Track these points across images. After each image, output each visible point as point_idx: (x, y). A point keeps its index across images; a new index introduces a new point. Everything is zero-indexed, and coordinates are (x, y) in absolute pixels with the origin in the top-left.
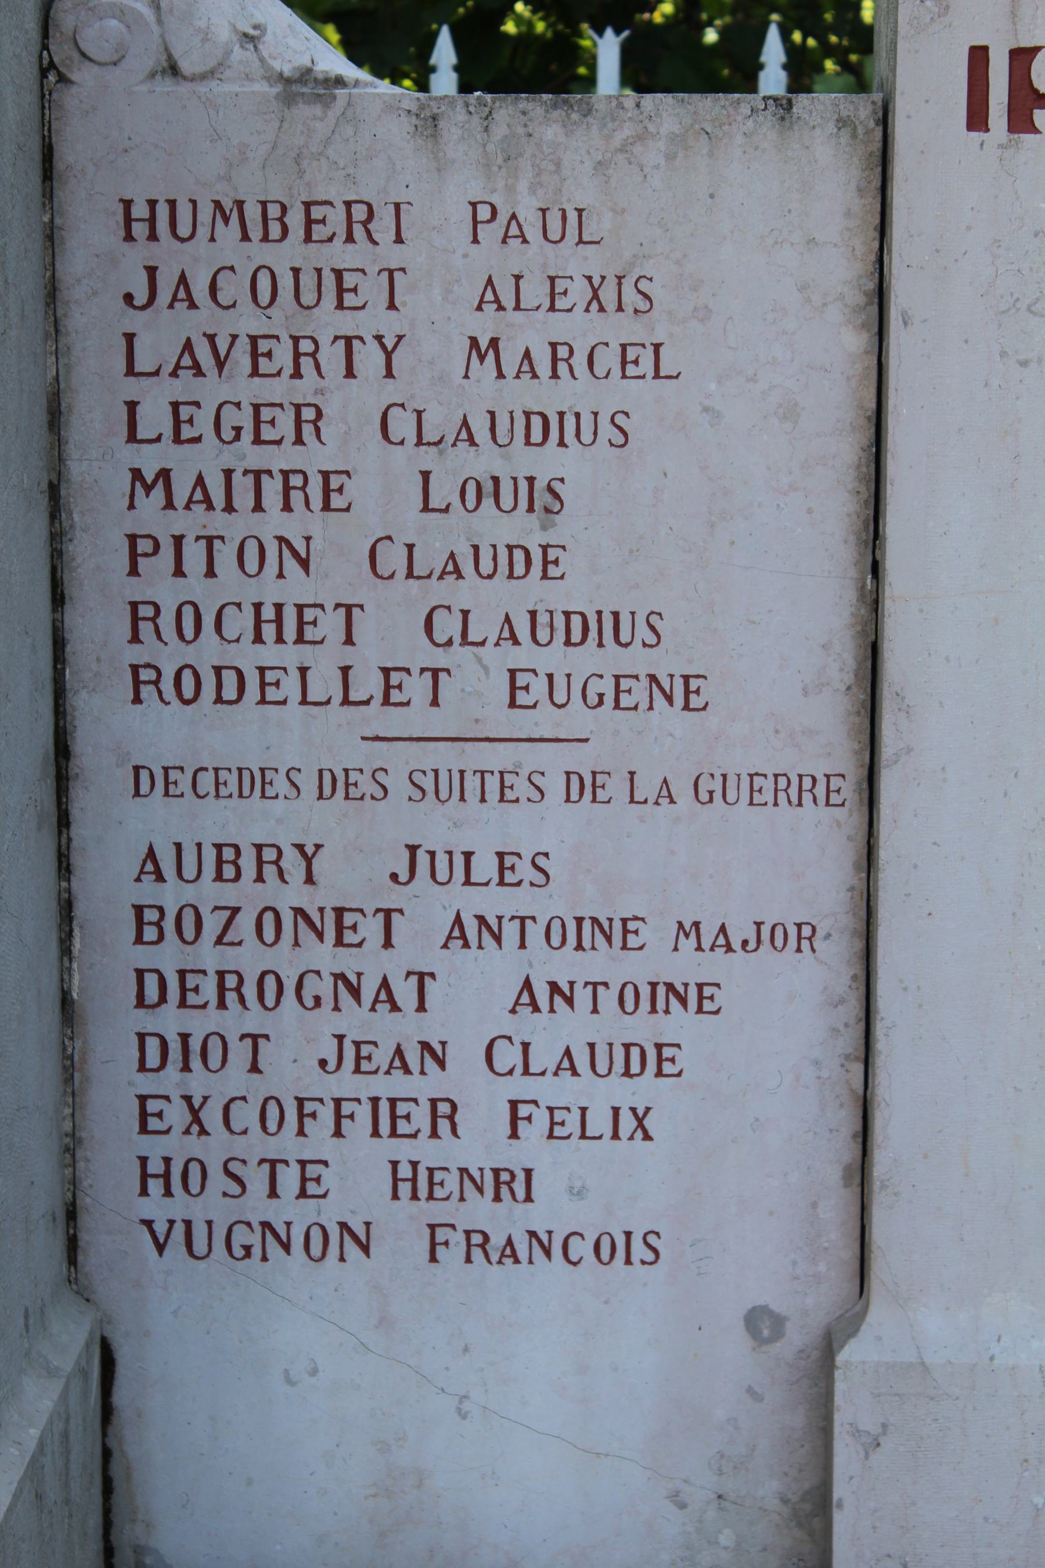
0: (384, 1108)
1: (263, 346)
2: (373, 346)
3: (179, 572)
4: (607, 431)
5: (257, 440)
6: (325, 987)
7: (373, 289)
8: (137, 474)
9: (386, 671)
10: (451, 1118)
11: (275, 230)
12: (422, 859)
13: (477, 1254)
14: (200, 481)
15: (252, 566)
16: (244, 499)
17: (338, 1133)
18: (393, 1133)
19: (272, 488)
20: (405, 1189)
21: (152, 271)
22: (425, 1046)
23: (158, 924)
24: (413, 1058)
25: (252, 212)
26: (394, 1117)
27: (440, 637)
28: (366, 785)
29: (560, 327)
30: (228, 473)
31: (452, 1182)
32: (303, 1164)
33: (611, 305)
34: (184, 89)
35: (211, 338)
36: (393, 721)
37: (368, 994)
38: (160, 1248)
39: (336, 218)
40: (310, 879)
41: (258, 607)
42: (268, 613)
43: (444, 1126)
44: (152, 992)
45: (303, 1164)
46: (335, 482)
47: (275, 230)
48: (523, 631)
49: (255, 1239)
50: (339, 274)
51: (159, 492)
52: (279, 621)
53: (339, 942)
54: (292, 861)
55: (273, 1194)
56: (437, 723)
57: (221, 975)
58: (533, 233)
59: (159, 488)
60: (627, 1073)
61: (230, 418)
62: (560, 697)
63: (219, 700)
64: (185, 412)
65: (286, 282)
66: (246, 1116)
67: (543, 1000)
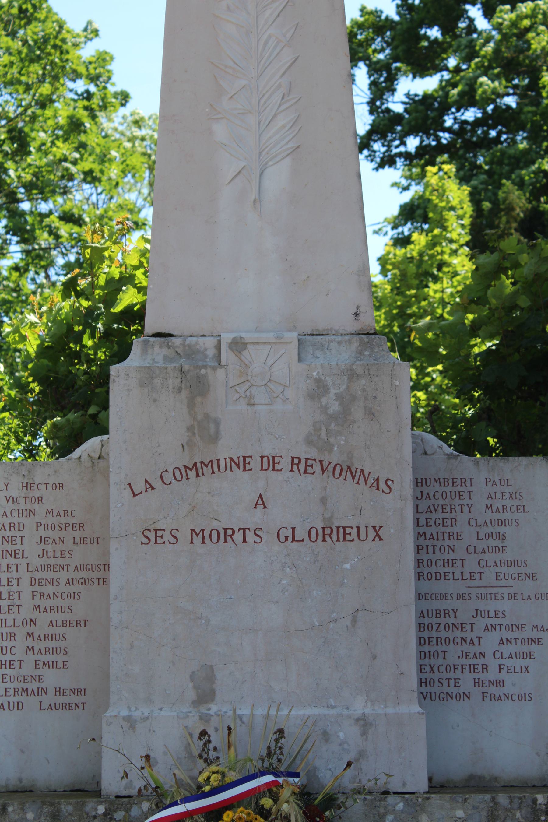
0: (472, 666)
1: (444, 507)
2: (466, 506)
3: (427, 553)
4: (514, 523)
5: (443, 526)
6: (459, 640)
7: (466, 495)
8: (419, 533)
9: (470, 573)
10: (486, 669)
11: (446, 484)
12: (479, 612)
13: (493, 699)
14: (432, 534)
15: (442, 551)
16: (441, 538)
17: (462, 672)
18: (474, 672)
19: (446, 535)
20: (477, 684)
21: (422, 492)
22: (480, 653)
23: (424, 627)
24: (478, 655)
25: (442, 480)
26: (474, 669)
27: (481, 566)
28: (467, 597)
29: (504, 502)
30: (437, 533)
31: (487, 683)
32: (455, 679)
33: (514, 498)
34: (428, 457)
35: (434, 505)
36: (472, 583)
37: (468, 642)
38: (425, 699)
39: (459, 481)
40: (455, 617)
41: (444, 560)
42: (446, 561)
43: (485, 670)
44: (422, 642)
45: (455, 679)
46: (459, 534)
47: (446, 484)
48: (498, 564)
49: (445, 696)
50: (459, 492)
51: (423, 536)
52: (448, 562)
53: (462, 631)
54: (452, 613)
55: (449, 686)
56: (481, 583)
57: (437, 638)
58: (498, 484)
59: (423, 536)
60: (523, 658)
61: (438, 521)
62: (507, 578)
63: (436, 579)
64: (428, 520)
65: (449, 494)
66: (443, 669)
67: (505, 642)
